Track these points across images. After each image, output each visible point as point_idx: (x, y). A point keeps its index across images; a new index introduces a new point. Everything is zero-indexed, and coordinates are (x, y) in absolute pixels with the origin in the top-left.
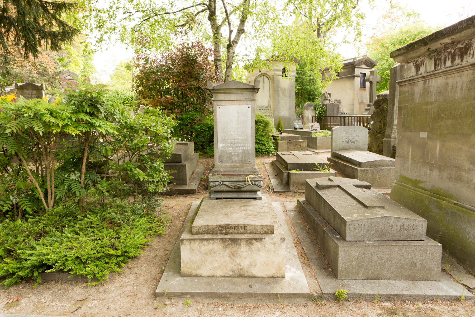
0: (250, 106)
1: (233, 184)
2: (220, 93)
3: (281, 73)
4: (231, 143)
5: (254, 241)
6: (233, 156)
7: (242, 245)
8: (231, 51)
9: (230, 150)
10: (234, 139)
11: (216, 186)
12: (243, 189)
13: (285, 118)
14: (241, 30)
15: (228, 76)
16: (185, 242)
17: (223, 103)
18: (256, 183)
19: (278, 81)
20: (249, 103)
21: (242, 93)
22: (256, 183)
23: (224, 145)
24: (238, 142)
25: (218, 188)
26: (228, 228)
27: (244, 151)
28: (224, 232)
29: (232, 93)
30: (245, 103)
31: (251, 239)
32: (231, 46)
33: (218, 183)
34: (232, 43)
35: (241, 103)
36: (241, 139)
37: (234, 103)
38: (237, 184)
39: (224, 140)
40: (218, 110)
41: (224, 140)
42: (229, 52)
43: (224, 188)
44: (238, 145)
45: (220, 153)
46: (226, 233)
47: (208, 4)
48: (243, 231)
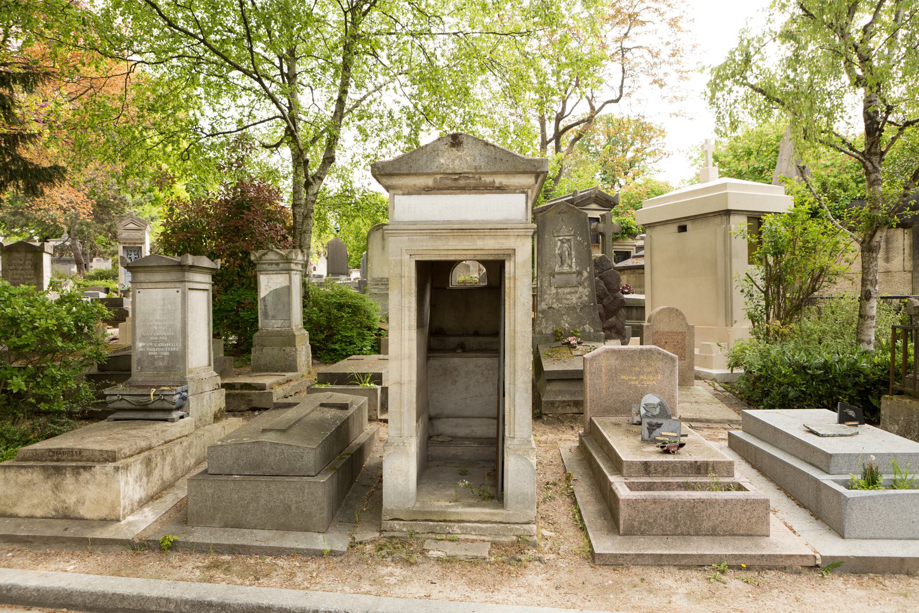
1: (135, 399)
2: (139, 272)
4: (153, 342)
5: (82, 470)
6: (156, 360)
9: (153, 352)
11: (114, 401)
12: (150, 406)
15: (305, 232)
17: (144, 285)
18: (166, 398)
20: (178, 285)
21: (168, 271)
22: (166, 398)
24: (164, 341)
25: (118, 405)
27: (171, 352)
28: (55, 458)
30: (172, 285)
31: (78, 467)
32: (311, 184)
33: (115, 398)
34: (311, 180)
35: (167, 285)
37: (159, 285)
39: (144, 338)
41: (144, 338)
43: (124, 405)
44: (162, 345)
45: (139, 356)
46: (58, 460)
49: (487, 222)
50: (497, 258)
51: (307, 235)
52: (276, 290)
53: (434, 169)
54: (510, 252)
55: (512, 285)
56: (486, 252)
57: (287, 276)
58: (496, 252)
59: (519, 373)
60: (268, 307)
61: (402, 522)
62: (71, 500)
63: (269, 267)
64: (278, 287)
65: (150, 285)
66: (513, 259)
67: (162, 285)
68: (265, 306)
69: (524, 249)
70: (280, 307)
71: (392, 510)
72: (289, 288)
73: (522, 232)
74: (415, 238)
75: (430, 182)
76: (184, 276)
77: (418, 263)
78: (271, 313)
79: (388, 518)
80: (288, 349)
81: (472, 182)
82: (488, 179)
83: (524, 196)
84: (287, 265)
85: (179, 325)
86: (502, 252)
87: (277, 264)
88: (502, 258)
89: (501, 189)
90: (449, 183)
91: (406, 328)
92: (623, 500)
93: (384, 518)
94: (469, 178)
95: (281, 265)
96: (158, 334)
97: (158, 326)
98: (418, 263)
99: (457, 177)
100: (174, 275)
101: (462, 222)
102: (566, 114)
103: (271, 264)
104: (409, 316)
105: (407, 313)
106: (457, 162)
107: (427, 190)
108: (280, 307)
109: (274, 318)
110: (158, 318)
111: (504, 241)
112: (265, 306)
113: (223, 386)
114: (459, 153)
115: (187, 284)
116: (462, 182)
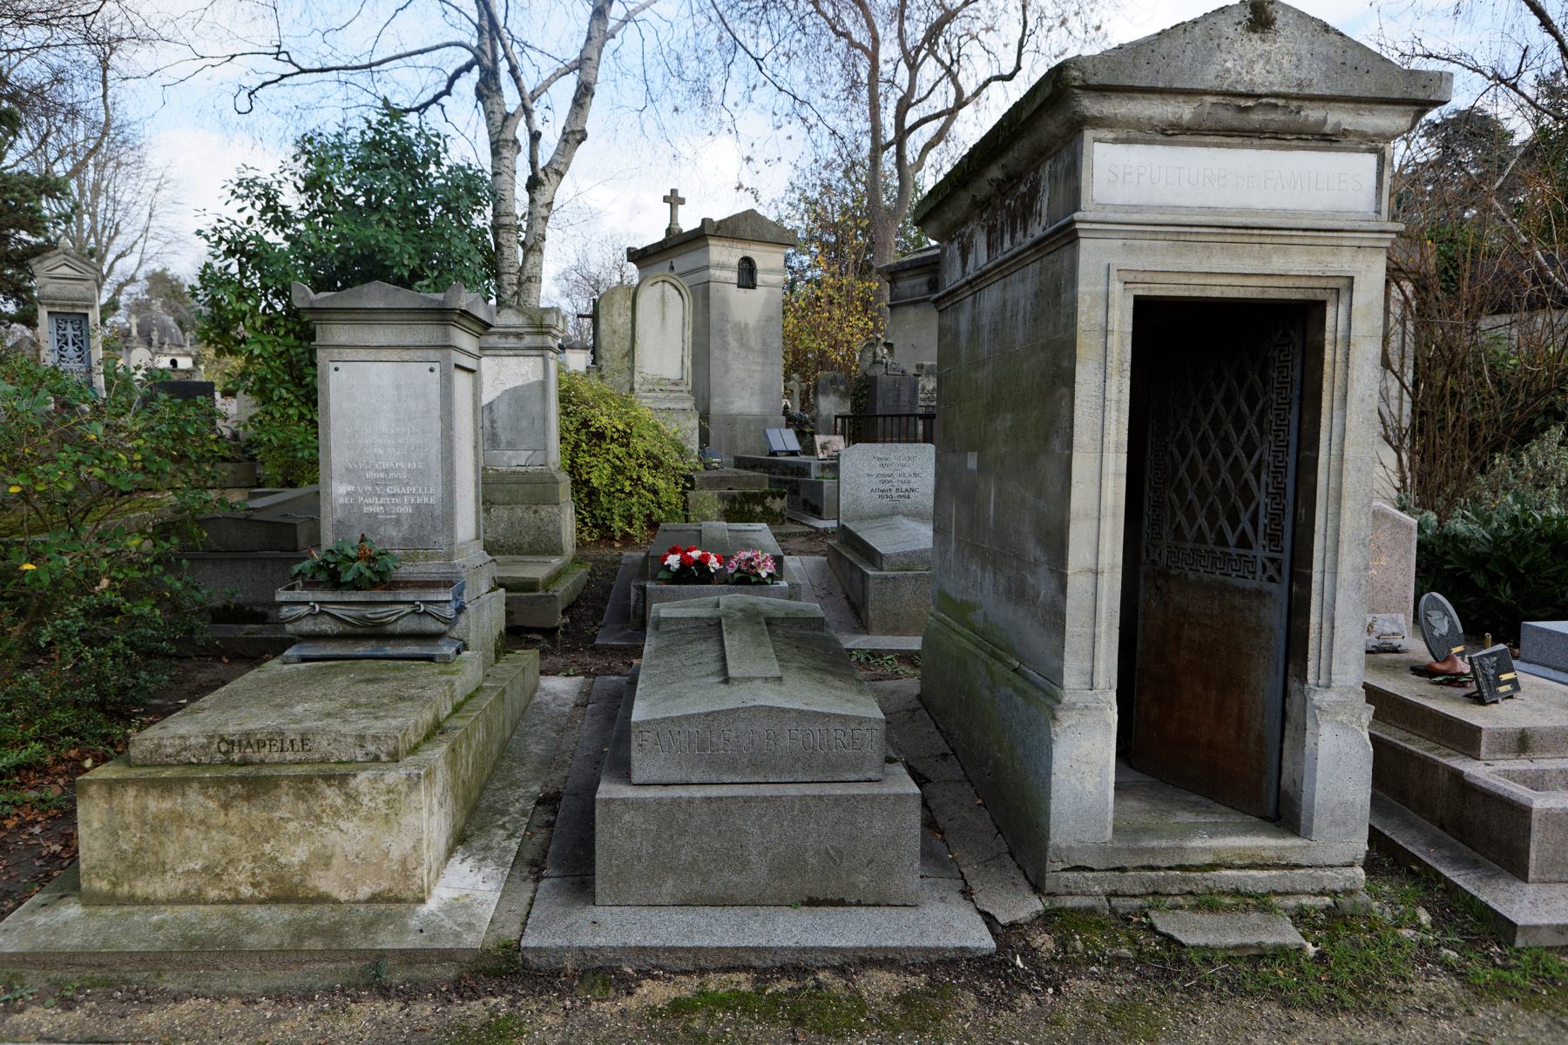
0: (436, 366)
1: (354, 612)
3: (733, 276)
4: (375, 483)
5: (322, 786)
6: (381, 523)
7: (284, 799)
8: (541, 199)
9: (373, 506)
10: (386, 471)
11: (300, 618)
12: (390, 628)
13: (748, 422)
14: (573, 132)
15: (529, 279)
16: (93, 790)
17: (349, 354)
18: (430, 608)
19: (725, 302)
20: (432, 354)
21: (409, 322)
22: (430, 608)
23: (351, 488)
24: (399, 482)
25: (307, 626)
26: (249, 745)
27: (417, 507)
28: (236, 757)
29: (380, 322)
31: (309, 779)
32: (541, 183)
33: (304, 610)
34: (541, 175)
35: (406, 355)
36: (409, 471)
37: (384, 354)
38: (369, 612)
39: (352, 474)
40: (333, 375)
41: (352, 474)
42: (532, 201)
43: (327, 626)
44: (396, 490)
45: (339, 514)
46: (244, 763)
47: (475, 43)
48: (301, 755)
49: (1295, 214)
50: (1310, 295)
51: (533, 286)
52: (516, 388)
53: (1208, 80)
54: (1341, 283)
55: (1339, 357)
56: (1290, 283)
57: (539, 360)
58: (1311, 283)
59: (1344, 548)
60: (499, 425)
61: (1089, 875)
62: (296, 855)
63: (502, 342)
64: (520, 383)
65: (363, 354)
66: (1344, 299)
67: (394, 354)
68: (493, 422)
69: (1370, 275)
70: (524, 423)
71: (1070, 848)
72: (544, 385)
73: (1369, 240)
74: (1137, 243)
75: (1184, 111)
76: (447, 335)
77: (1137, 298)
78: (504, 437)
79: (1060, 866)
80: (545, 511)
81: (1278, 117)
82: (1313, 114)
83: (1372, 159)
84: (538, 341)
85: (435, 448)
86: (1323, 283)
87: (519, 336)
88: (1320, 297)
89: (1328, 139)
90: (1229, 117)
91: (1112, 449)
92: (1539, 811)
93: (1049, 866)
94: (1276, 106)
95: (528, 340)
96: (386, 465)
97: (385, 447)
98: (1139, 301)
99: (1250, 103)
100: (425, 333)
101: (1240, 212)
102: (916, 97)
103: (506, 335)
104: (1118, 422)
105: (1114, 414)
106: (1258, 67)
107: (1171, 133)
108: (524, 423)
109: (511, 446)
110: (384, 429)
111: (1330, 258)
112: (493, 422)
113: (499, 584)
114: (1266, 47)
115: (454, 354)
116: (1257, 118)
